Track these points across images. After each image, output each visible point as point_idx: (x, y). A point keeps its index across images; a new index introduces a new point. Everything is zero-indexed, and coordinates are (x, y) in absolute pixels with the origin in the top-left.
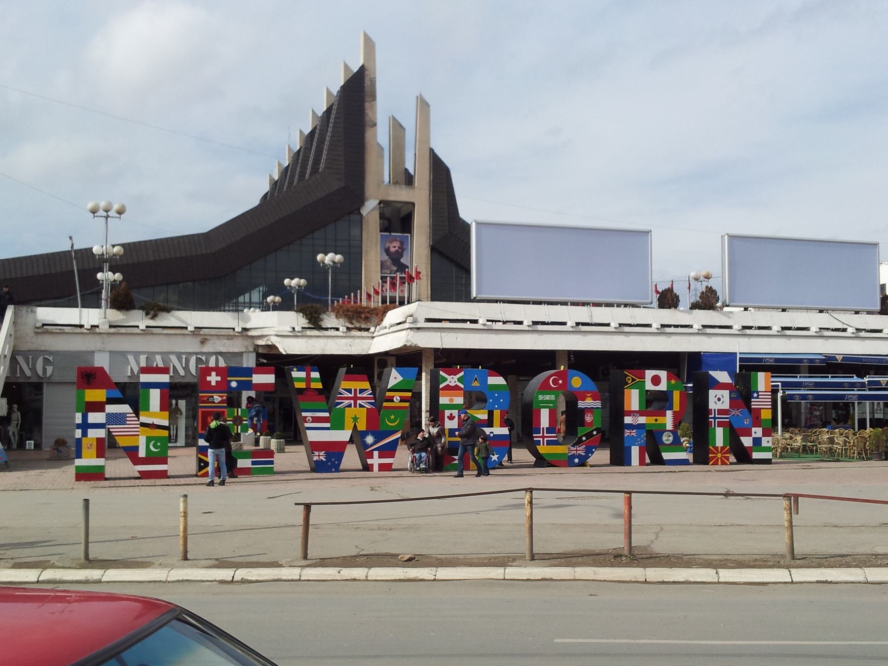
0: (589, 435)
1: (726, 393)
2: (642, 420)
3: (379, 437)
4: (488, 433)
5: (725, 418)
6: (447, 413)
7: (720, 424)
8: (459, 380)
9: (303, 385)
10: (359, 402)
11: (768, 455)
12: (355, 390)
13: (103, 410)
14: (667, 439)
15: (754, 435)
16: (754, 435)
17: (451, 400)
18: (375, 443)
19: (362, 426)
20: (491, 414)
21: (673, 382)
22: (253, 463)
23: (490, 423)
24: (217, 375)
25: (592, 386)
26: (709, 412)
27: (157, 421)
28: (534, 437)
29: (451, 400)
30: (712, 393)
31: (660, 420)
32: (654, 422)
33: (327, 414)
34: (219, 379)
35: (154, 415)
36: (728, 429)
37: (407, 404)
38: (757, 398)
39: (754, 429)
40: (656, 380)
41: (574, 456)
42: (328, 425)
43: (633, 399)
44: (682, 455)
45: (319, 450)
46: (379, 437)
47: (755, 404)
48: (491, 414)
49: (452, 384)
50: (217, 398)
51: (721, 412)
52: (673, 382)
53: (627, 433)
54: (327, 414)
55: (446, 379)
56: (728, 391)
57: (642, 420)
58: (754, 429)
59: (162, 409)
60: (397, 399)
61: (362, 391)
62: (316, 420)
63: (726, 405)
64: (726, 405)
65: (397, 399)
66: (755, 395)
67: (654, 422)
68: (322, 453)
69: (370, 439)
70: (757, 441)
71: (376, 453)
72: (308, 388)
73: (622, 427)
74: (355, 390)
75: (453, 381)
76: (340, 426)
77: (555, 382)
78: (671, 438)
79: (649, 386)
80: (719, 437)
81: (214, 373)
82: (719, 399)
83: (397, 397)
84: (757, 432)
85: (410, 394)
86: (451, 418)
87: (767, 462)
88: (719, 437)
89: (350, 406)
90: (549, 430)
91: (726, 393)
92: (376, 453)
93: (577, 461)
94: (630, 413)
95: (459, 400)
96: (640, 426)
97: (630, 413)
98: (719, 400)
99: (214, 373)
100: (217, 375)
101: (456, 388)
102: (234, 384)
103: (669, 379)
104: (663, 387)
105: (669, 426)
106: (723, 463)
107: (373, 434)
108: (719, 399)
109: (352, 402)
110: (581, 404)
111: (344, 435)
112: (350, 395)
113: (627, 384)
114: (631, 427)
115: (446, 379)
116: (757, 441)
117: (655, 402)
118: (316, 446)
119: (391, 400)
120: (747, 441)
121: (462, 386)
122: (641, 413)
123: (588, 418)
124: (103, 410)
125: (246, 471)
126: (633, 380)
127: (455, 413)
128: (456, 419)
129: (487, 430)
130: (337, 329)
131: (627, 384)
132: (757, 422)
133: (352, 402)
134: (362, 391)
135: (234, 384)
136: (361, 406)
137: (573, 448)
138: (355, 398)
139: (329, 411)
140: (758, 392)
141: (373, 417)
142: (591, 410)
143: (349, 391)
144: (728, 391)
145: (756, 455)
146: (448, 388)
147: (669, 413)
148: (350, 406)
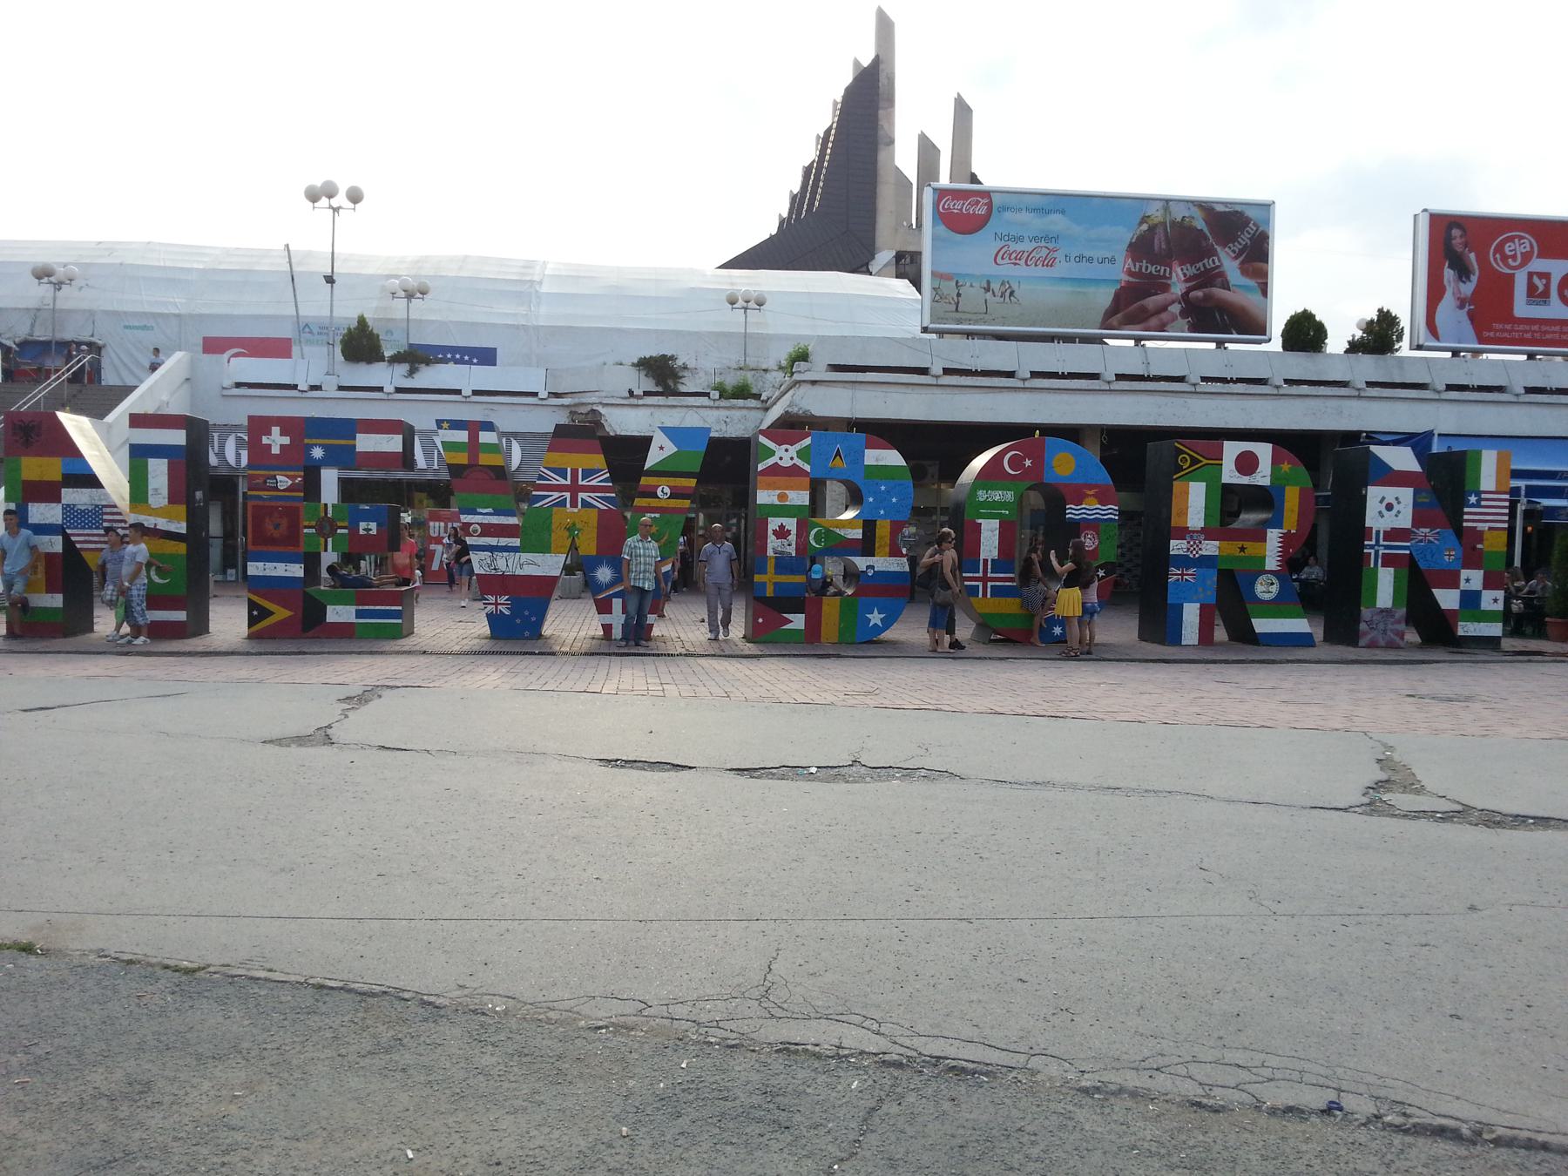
1: (1406, 494)
2: (1210, 548)
5: (1402, 548)
6: (774, 523)
7: (1388, 561)
8: (800, 454)
9: (462, 459)
10: (581, 495)
11: (1495, 629)
12: (575, 472)
13: (58, 499)
14: (1266, 589)
15: (1463, 585)
17: (782, 497)
19: (588, 547)
20: (869, 526)
21: (1286, 467)
22: (359, 614)
24: (282, 434)
26: (1364, 532)
27: (163, 524)
30: (1375, 495)
31: (1252, 548)
32: (1237, 553)
34: (286, 440)
35: (156, 512)
36: (1405, 572)
38: (1478, 505)
39: (1464, 573)
40: (1247, 463)
42: (516, 542)
44: (1300, 625)
45: (497, 594)
47: (1471, 517)
49: (786, 463)
50: (283, 481)
51: (1393, 534)
52: (1286, 467)
53: (1174, 575)
55: (773, 453)
57: (1210, 548)
58: (1464, 573)
59: (173, 499)
60: (663, 491)
62: (487, 530)
63: (1405, 521)
64: (1405, 521)
65: (663, 491)
66: (1473, 499)
67: (1237, 553)
68: (503, 599)
70: (1470, 600)
72: (473, 465)
73: (1160, 561)
74: (575, 472)
75: (786, 456)
76: (544, 548)
78: (1275, 589)
79: (1230, 475)
80: (1385, 587)
81: (276, 430)
82: (1389, 507)
84: (1473, 578)
85: (692, 482)
87: (1491, 643)
88: (1385, 587)
89: (562, 503)
90: (997, 565)
91: (1406, 494)
94: (1183, 533)
98: (1388, 509)
99: (276, 430)
100: (282, 434)
101: (794, 471)
103: (1276, 461)
105: (1272, 563)
106: (1391, 646)
108: (1389, 507)
109: (568, 495)
110: (1073, 512)
111: (549, 564)
112: (563, 482)
114: (1184, 561)
115: (773, 453)
116: (1470, 600)
118: (492, 585)
120: (1447, 599)
121: (807, 468)
122: (1207, 533)
124: (58, 499)
125: (344, 632)
126: (1194, 461)
127: (791, 524)
128: (793, 537)
130: (707, 395)
133: (568, 495)
134: (588, 473)
135: (318, 453)
136: (586, 504)
138: (574, 489)
140: (1478, 493)
142: (1094, 525)
145: (1466, 629)
146: (775, 470)
147: (1274, 536)
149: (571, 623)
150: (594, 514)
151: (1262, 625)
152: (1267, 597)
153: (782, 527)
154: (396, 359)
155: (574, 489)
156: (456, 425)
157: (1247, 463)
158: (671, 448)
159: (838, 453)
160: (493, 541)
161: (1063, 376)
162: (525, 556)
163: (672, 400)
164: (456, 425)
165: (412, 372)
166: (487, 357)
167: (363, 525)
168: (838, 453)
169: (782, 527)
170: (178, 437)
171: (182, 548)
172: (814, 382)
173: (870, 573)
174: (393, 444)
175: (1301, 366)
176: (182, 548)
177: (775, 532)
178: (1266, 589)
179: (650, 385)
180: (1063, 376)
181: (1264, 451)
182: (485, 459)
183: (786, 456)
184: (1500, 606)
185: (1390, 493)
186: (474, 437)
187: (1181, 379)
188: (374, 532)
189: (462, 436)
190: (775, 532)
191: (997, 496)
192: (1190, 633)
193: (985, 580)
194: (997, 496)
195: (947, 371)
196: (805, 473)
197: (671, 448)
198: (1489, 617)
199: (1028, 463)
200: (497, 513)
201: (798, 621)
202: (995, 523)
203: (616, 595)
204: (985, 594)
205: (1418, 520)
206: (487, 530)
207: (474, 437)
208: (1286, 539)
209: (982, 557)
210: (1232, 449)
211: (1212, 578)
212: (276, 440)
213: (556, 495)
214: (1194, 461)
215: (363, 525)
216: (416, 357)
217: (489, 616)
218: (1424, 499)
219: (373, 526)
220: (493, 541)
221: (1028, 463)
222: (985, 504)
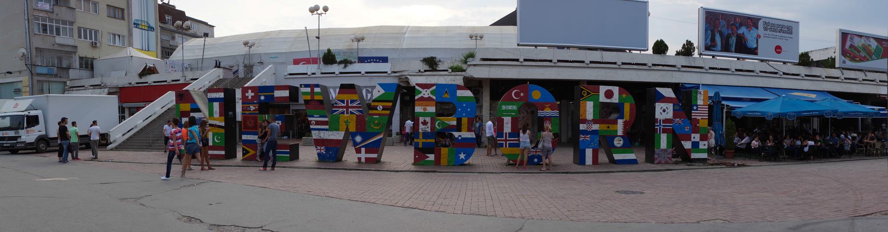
1: (670, 106)
2: (596, 127)
3: (366, 137)
4: (456, 136)
6: (421, 119)
7: (664, 131)
8: (431, 92)
9: (309, 98)
11: (704, 156)
14: (618, 142)
15: (693, 140)
16: (693, 140)
19: (353, 129)
20: (459, 121)
21: (624, 96)
23: (458, 128)
25: (551, 98)
27: (218, 123)
29: (425, 109)
30: (659, 106)
31: (612, 127)
35: (215, 119)
37: (388, 112)
39: (693, 135)
40: (609, 94)
42: (327, 127)
43: (589, 109)
44: (631, 156)
46: (366, 137)
47: (695, 115)
48: (459, 121)
49: (426, 96)
50: (252, 108)
51: (666, 121)
52: (624, 96)
55: (421, 92)
56: (671, 105)
57: (596, 127)
58: (693, 135)
59: (220, 116)
60: (380, 108)
61: (352, 101)
62: (318, 123)
63: (670, 115)
64: (670, 115)
65: (380, 108)
68: (323, 148)
69: (358, 139)
70: (695, 145)
71: (363, 150)
72: (312, 100)
73: (577, 132)
77: (517, 94)
78: (622, 142)
79: (602, 99)
80: (664, 141)
84: (696, 137)
85: (390, 104)
88: (664, 141)
89: (343, 113)
90: (511, 135)
91: (670, 106)
92: (363, 150)
93: (536, 160)
94: (585, 121)
95: (432, 109)
96: (595, 132)
97: (585, 121)
98: (663, 111)
101: (429, 99)
102: (262, 98)
103: (620, 93)
104: (615, 99)
105: (620, 133)
107: (361, 135)
108: (664, 111)
110: (541, 113)
111: (339, 135)
113: (582, 96)
114: (585, 132)
115: (421, 92)
116: (695, 145)
117: (607, 112)
118: (318, 143)
119: (375, 108)
120: (687, 145)
122: (595, 121)
126: (588, 93)
127: (428, 119)
128: (429, 125)
129: (456, 134)
131: (582, 96)
132: (696, 130)
134: (352, 101)
136: (351, 113)
138: (347, 107)
140: (697, 106)
141: (361, 122)
142: (549, 118)
143: (343, 101)
144: (671, 105)
145: (694, 156)
148: (343, 113)
149: (350, 156)
151: (617, 157)
152: (619, 145)
154: (340, 63)
155: (347, 107)
156: (306, 86)
157: (609, 94)
158: (382, 91)
160: (319, 127)
161: (570, 62)
162: (330, 133)
163: (435, 73)
164: (306, 86)
165: (345, 67)
166: (385, 60)
170: (221, 95)
171: (223, 131)
172: (475, 65)
174: (286, 93)
175: (658, 59)
176: (223, 131)
178: (618, 142)
179: (427, 68)
180: (570, 62)
181: (616, 90)
182: (317, 98)
184: (706, 147)
185: (664, 105)
186: (312, 90)
187: (615, 63)
189: (308, 90)
191: (510, 107)
192: (589, 159)
193: (506, 140)
194: (510, 107)
195: (525, 60)
196: (433, 100)
197: (382, 91)
198: (702, 151)
200: (321, 117)
201: (431, 157)
202: (510, 118)
205: (675, 116)
206: (318, 123)
207: (312, 90)
208: (625, 123)
210: (603, 89)
211: (597, 139)
212: (250, 94)
214: (588, 93)
216: (346, 62)
217: (318, 154)
218: (677, 108)
220: (319, 127)
222: (506, 111)
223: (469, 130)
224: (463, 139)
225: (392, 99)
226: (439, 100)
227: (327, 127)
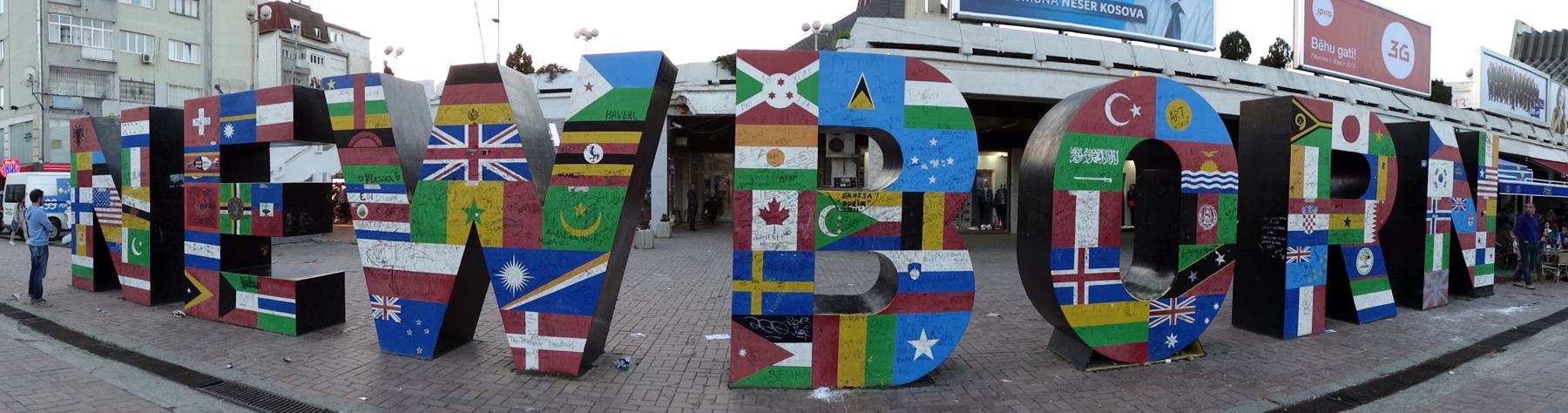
0: (1206, 267)
3: (543, 267)
6: (761, 199)
8: (803, 88)
10: (482, 162)
17: (774, 157)
18: (528, 288)
20: (913, 203)
28: (1052, 279)
29: (774, 157)
33: (402, 199)
37: (627, 170)
41: (1164, 330)
42: (404, 228)
46: (541, 271)
49: (780, 103)
54: (402, 199)
55: (758, 87)
69: (514, 275)
71: (532, 319)
75: (781, 92)
76: (438, 237)
77: (1120, 109)
83: (594, 147)
85: (634, 137)
86: (774, 215)
89: (457, 175)
92: (532, 319)
95: (802, 157)
101: (794, 115)
107: (523, 259)
109: (465, 162)
112: (459, 145)
115: (758, 87)
121: (814, 110)
122: (1320, 206)
123: (1206, 219)
127: (789, 200)
128: (791, 224)
133: (465, 162)
134: (491, 131)
136: (488, 175)
137: (1163, 307)
139: (410, 189)
141: (524, 206)
143: (457, 132)
148: (457, 175)
150: (499, 185)
153: (774, 205)
155: (474, 154)
159: (862, 87)
160: (385, 226)
167: (262, 206)
168: (862, 87)
169: (774, 205)
173: (915, 275)
177: (764, 214)
183: (781, 92)
188: (271, 214)
190: (764, 214)
191: (1097, 156)
193: (1081, 278)
194: (1097, 156)
197: (603, 87)
199: (1136, 111)
200: (384, 190)
201: (800, 354)
202: (1096, 194)
203: (531, 307)
204: (1081, 301)
206: (378, 212)
209: (1077, 247)
213: (451, 163)
215: (262, 206)
219: (270, 206)
220: (385, 226)
221: (1136, 111)
222: (1079, 168)
223: (952, 241)
224: (926, 276)
225: (641, 116)
226: (828, 121)
227: (404, 228)
